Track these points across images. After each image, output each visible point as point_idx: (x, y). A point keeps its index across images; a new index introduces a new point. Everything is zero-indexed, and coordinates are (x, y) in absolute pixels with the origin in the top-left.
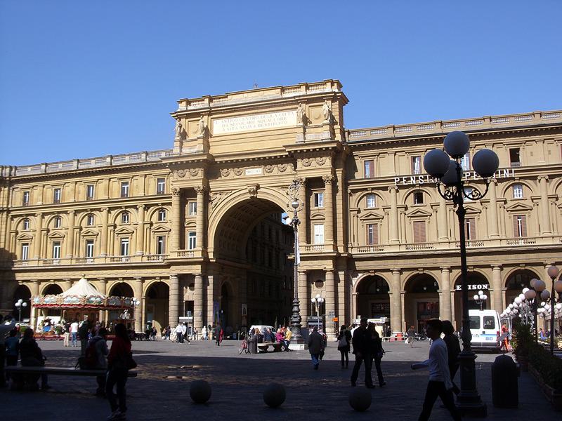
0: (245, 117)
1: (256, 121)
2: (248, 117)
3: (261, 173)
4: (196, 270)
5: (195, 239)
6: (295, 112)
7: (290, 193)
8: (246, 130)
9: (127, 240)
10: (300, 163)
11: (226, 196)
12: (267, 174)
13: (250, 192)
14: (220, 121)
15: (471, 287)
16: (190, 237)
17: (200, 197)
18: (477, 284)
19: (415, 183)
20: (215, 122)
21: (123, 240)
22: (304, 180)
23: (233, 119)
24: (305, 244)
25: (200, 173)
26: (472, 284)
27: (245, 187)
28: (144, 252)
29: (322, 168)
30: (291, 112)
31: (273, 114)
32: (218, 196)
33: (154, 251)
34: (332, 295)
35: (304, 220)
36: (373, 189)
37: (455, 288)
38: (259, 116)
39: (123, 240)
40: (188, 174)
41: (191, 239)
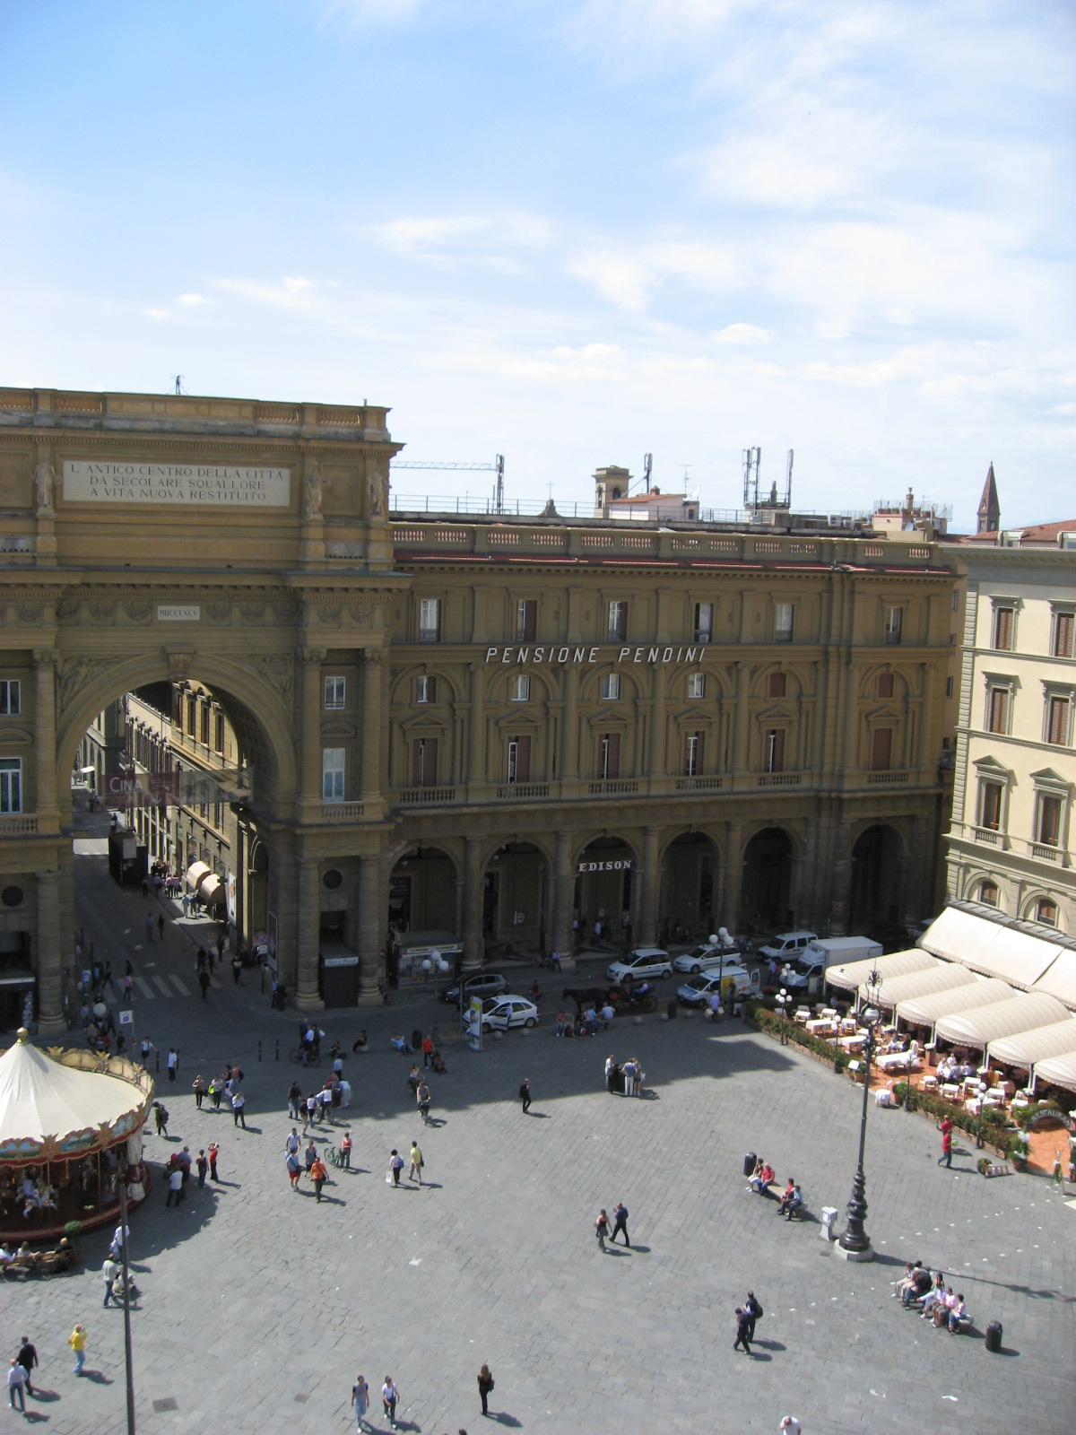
0: (154, 467)
1: (185, 480)
2: (164, 467)
3: (197, 617)
5: (15, 778)
6: (286, 472)
8: (158, 500)
10: (312, 617)
15: (604, 866)
18: (614, 860)
19: (524, 660)
20: (67, 465)
22: (323, 655)
23: (122, 466)
25: (49, 614)
26: (605, 861)
30: (276, 471)
31: (231, 470)
32: (83, 671)
38: (194, 469)
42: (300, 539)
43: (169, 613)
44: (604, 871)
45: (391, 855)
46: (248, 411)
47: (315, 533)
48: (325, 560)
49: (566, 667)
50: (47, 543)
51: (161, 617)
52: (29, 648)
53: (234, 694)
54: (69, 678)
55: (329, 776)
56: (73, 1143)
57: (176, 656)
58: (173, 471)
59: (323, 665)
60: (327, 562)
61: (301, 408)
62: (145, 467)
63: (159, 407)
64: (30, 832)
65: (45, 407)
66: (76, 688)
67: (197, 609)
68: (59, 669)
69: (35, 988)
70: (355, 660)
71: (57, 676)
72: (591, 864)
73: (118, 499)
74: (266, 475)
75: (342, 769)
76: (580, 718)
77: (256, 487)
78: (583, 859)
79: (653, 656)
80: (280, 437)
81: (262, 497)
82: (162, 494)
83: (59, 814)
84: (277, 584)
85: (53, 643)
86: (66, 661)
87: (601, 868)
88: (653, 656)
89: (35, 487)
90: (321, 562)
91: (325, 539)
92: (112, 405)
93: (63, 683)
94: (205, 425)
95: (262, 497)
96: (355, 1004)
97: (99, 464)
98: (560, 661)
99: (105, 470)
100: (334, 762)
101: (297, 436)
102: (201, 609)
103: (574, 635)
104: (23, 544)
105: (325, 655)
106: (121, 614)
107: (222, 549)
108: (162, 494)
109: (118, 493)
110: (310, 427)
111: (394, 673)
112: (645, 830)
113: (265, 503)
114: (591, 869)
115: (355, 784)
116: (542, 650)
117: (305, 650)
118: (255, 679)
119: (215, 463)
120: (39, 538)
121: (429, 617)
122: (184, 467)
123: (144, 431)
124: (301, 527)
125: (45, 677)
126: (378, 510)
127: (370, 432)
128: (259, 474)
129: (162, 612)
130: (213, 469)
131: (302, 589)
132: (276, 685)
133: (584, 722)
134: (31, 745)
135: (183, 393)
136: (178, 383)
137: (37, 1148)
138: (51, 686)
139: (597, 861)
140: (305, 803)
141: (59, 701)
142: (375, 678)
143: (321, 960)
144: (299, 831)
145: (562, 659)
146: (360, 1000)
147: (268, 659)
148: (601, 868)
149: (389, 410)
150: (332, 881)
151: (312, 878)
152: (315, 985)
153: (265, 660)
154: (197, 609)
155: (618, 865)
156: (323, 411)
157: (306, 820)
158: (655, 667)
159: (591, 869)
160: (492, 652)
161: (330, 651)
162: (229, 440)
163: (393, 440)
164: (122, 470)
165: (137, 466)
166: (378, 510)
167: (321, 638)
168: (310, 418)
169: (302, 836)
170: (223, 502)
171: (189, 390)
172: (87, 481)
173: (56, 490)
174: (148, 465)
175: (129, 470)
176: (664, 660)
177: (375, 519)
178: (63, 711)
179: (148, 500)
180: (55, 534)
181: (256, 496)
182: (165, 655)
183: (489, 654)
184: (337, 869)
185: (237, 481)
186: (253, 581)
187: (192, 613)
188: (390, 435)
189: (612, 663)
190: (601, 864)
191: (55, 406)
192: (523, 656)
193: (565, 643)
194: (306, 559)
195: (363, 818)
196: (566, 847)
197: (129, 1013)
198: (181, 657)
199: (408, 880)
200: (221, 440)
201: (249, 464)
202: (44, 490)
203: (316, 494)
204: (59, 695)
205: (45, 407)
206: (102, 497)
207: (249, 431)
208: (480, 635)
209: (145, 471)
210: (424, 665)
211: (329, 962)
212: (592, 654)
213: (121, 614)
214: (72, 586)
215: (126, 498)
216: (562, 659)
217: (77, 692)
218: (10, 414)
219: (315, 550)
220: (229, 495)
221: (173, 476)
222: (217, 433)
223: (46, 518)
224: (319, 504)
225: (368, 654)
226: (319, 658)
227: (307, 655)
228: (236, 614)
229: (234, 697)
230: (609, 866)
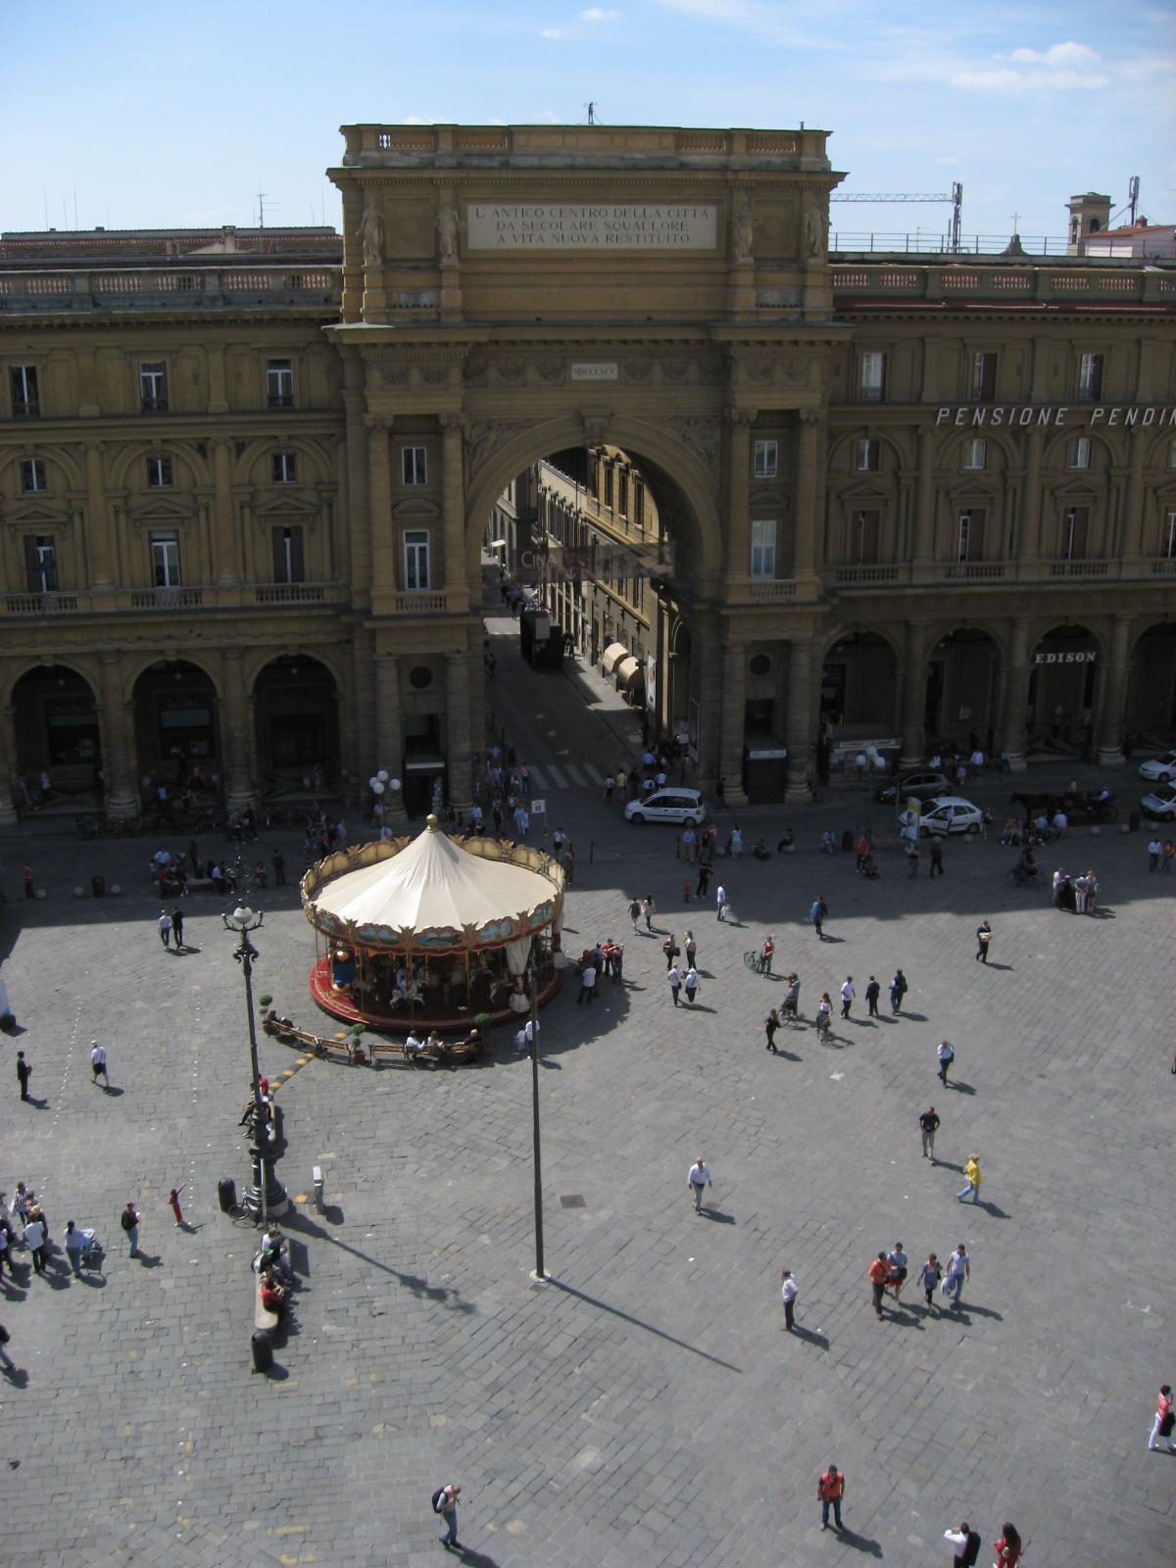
2: (576, 208)
3: (614, 376)
6: (712, 210)
8: (570, 245)
10: (741, 374)
14: (487, 210)
15: (1065, 657)
16: (406, 546)
18: (1076, 650)
19: (980, 422)
20: (472, 209)
23: (531, 208)
25: (455, 375)
26: (1066, 651)
30: (700, 209)
31: (651, 210)
32: (492, 436)
37: (1034, 659)
38: (610, 209)
39: (156, 537)
40: (415, 376)
41: (411, 551)
42: (728, 286)
44: (1065, 664)
45: (824, 639)
46: (669, 141)
47: (745, 278)
48: (756, 309)
49: (1029, 431)
50: (452, 297)
51: (575, 377)
52: (433, 412)
53: (655, 460)
54: (477, 445)
55: (758, 551)
56: (432, 939)
57: (592, 419)
58: (587, 213)
59: (752, 428)
60: (757, 312)
61: (728, 136)
62: (556, 208)
63: (571, 140)
64: (438, 610)
65: (446, 144)
66: (486, 455)
67: (615, 366)
68: (467, 436)
69: (444, 774)
70: (789, 422)
71: (465, 443)
72: (1049, 656)
73: (527, 245)
74: (690, 214)
75: (773, 545)
76: (937, 491)
77: (679, 227)
78: (1040, 649)
79: (1131, 417)
80: (706, 169)
81: (685, 238)
82: (575, 238)
83: (467, 590)
84: (700, 336)
85: (460, 406)
86: (473, 426)
87: (1061, 660)
88: (1131, 417)
89: (438, 235)
90: (752, 312)
91: (757, 285)
92: (520, 140)
93: (471, 449)
94: (622, 159)
95: (685, 238)
96: (780, 799)
97: (506, 207)
98: (1021, 423)
99: (512, 213)
100: (764, 535)
101: (724, 168)
102: (619, 368)
103: (1039, 393)
104: (426, 298)
105: (755, 417)
106: (532, 375)
107: (641, 299)
108: (575, 238)
109: (527, 239)
110: (740, 157)
111: (832, 437)
112: (1113, 619)
113: (689, 246)
114: (1049, 661)
115: (786, 562)
116: (1002, 410)
117: (733, 412)
119: (631, 202)
120: (443, 292)
121: (872, 373)
122: (598, 207)
123: (557, 169)
124: (728, 272)
125: (452, 444)
126: (816, 251)
127: (807, 162)
128: (682, 213)
129: (579, 371)
130: (630, 208)
131: (730, 343)
132: (701, 450)
133: (941, 495)
134: (438, 519)
135: (596, 123)
136: (591, 112)
137: (394, 937)
138: (459, 453)
139: (1056, 651)
140: (730, 582)
141: (467, 471)
142: (811, 442)
143: (746, 753)
144: (724, 612)
145: (1025, 420)
146: (787, 796)
147: (692, 422)
148: (1061, 660)
149: (829, 133)
150: (759, 665)
151: (738, 663)
152: (738, 778)
153: (688, 423)
154: (615, 366)
155: (1080, 657)
156: (754, 138)
157: (732, 600)
158: (1133, 430)
159: (1049, 661)
160: (944, 412)
161: (761, 413)
162: (648, 175)
163: (835, 168)
164: (529, 213)
165: (547, 208)
166: (816, 251)
167: (751, 397)
168: (739, 146)
169: (728, 617)
170: (642, 245)
171: (604, 118)
172: (494, 227)
173: (460, 237)
174: (559, 207)
175: (539, 213)
176: (1144, 423)
177: (812, 261)
178: (471, 480)
179: (560, 246)
180: (461, 287)
181: (678, 238)
182: (580, 419)
183: (940, 415)
185: (657, 225)
187: (609, 371)
188: (830, 163)
189: (1082, 427)
190: (1061, 655)
191: (456, 144)
192: (979, 418)
193: (1028, 403)
194: (735, 309)
195: (794, 598)
196: (1022, 636)
197: (542, 803)
198: (598, 420)
199: (843, 668)
200: (639, 175)
201: (671, 202)
202: (448, 238)
203: (746, 235)
204: (467, 464)
205: (446, 144)
206: (510, 244)
207: (671, 164)
208: (930, 394)
209: (556, 213)
210: (866, 428)
211: (754, 755)
212: (1059, 415)
213: (532, 375)
214: (479, 344)
215: (535, 245)
216: (1025, 420)
217: (487, 459)
218: (408, 155)
219: (745, 298)
220: (648, 239)
221: (587, 218)
222: (635, 168)
223: (450, 269)
224: (749, 245)
225: (803, 416)
226: (748, 421)
227: (735, 417)
229: (654, 464)
230: (1070, 658)
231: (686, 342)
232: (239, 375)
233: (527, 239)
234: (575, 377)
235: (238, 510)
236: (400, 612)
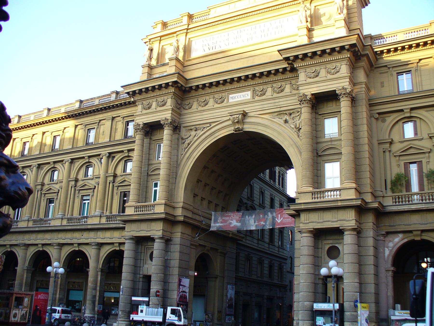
4: (156, 230)
7: (290, 121)
9: (88, 198)
11: (203, 132)
12: (257, 98)
13: (234, 123)
16: (154, 189)
17: (167, 132)
21: (85, 198)
24: (311, 189)
25: (170, 102)
27: (227, 118)
28: (105, 212)
29: (336, 77)
32: (193, 133)
33: (115, 211)
34: (354, 268)
35: (306, 155)
36: (412, 109)
39: (85, 198)
40: (154, 105)
43: (235, 97)
57: (233, 116)
118: (280, 125)
153: (286, 114)
184: (336, 245)
186: (272, 68)
187: (246, 95)
198: (235, 116)
213: (211, 102)
217: (189, 144)
228: (269, 92)
231: (277, 71)
232: (116, 129)
233: (214, 48)
234: (231, 100)
235: (108, 184)
236: (135, 213)
